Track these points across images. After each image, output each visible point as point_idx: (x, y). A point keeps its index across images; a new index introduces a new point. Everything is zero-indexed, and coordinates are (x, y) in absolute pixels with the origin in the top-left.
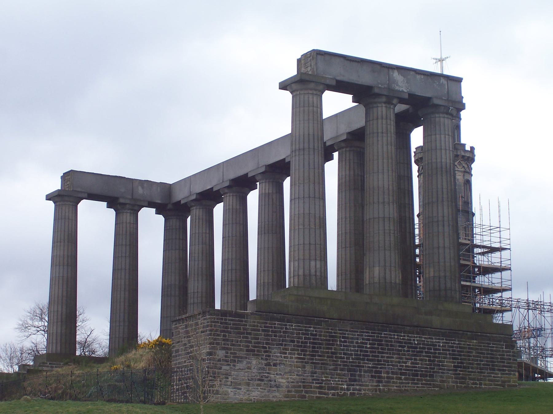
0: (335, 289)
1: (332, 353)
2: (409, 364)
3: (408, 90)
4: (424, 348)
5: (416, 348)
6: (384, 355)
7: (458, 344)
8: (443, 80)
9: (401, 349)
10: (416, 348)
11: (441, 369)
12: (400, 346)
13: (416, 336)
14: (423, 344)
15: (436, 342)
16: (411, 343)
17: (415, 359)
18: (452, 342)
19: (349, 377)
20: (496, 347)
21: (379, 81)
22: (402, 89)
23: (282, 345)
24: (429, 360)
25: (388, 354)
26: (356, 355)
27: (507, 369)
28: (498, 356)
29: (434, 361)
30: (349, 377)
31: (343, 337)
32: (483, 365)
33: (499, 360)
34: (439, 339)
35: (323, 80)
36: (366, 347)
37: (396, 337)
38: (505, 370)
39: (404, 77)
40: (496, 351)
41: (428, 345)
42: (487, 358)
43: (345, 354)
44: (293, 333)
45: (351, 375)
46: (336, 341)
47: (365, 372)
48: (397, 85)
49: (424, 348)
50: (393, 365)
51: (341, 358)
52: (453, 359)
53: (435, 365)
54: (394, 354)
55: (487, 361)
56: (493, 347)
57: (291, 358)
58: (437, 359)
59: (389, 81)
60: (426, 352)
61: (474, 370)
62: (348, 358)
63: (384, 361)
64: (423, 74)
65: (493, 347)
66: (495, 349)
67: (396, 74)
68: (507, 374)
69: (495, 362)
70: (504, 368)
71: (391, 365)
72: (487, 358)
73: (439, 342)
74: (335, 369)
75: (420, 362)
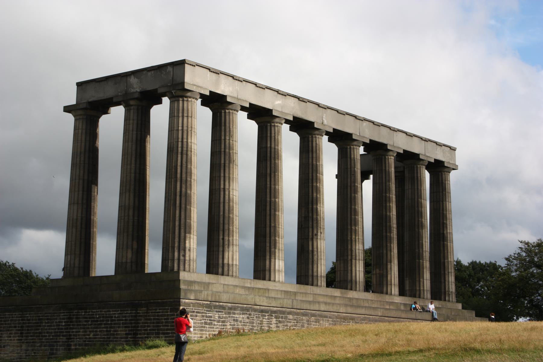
0: (111, 271)
1: (40, 333)
2: (91, 336)
3: (141, 89)
4: (103, 321)
5: (97, 321)
6: (74, 330)
7: (130, 313)
8: (170, 69)
9: (86, 324)
10: (97, 321)
11: (115, 338)
12: (86, 321)
13: (98, 310)
14: (103, 317)
15: (112, 314)
16: (93, 318)
17: (96, 331)
18: (125, 312)
19: (50, 351)
20: (162, 312)
21: (119, 91)
22: (136, 90)
23: (9, 330)
24: (107, 331)
25: (76, 329)
26: (55, 332)
27: (170, 331)
28: (163, 321)
29: (110, 331)
30: (50, 351)
31: (47, 319)
32: (150, 330)
33: (164, 324)
34: (115, 311)
35: (81, 106)
36: (62, 325)
37: (83, 314)
38: (168, 333)
39: (138, 79)
40: (162, 316)
41: (107, 317)
42: (154, 323)
43: (47, 333)
44: (15, 320)
45: (52, 350)
46: (42, 323)
47: (60, 346)
48: (133, 88)
49: (103, 321)
50: (79, 338)
51: (45, 336)
52: (125, 327)
53: (111, 335)
54: (81, 328)
55: (153, 326)
56: (159, 312)
57: (14, 340)
58: (112, 329)
59: (126, 87)
60: (105, 324)
61: (142, 336)
62: (49, 336)
63: (74, 335)
64: (154, 70)
65: (159, 312)
66: (161, 314)
67: (133, 80)
68: (170, 337)
69: (160, 326)
70: (168, 331)
71: (78, 338)
72: (154, 323)
73: (115, 314)
74: (40, 346)
75: (100, 333)
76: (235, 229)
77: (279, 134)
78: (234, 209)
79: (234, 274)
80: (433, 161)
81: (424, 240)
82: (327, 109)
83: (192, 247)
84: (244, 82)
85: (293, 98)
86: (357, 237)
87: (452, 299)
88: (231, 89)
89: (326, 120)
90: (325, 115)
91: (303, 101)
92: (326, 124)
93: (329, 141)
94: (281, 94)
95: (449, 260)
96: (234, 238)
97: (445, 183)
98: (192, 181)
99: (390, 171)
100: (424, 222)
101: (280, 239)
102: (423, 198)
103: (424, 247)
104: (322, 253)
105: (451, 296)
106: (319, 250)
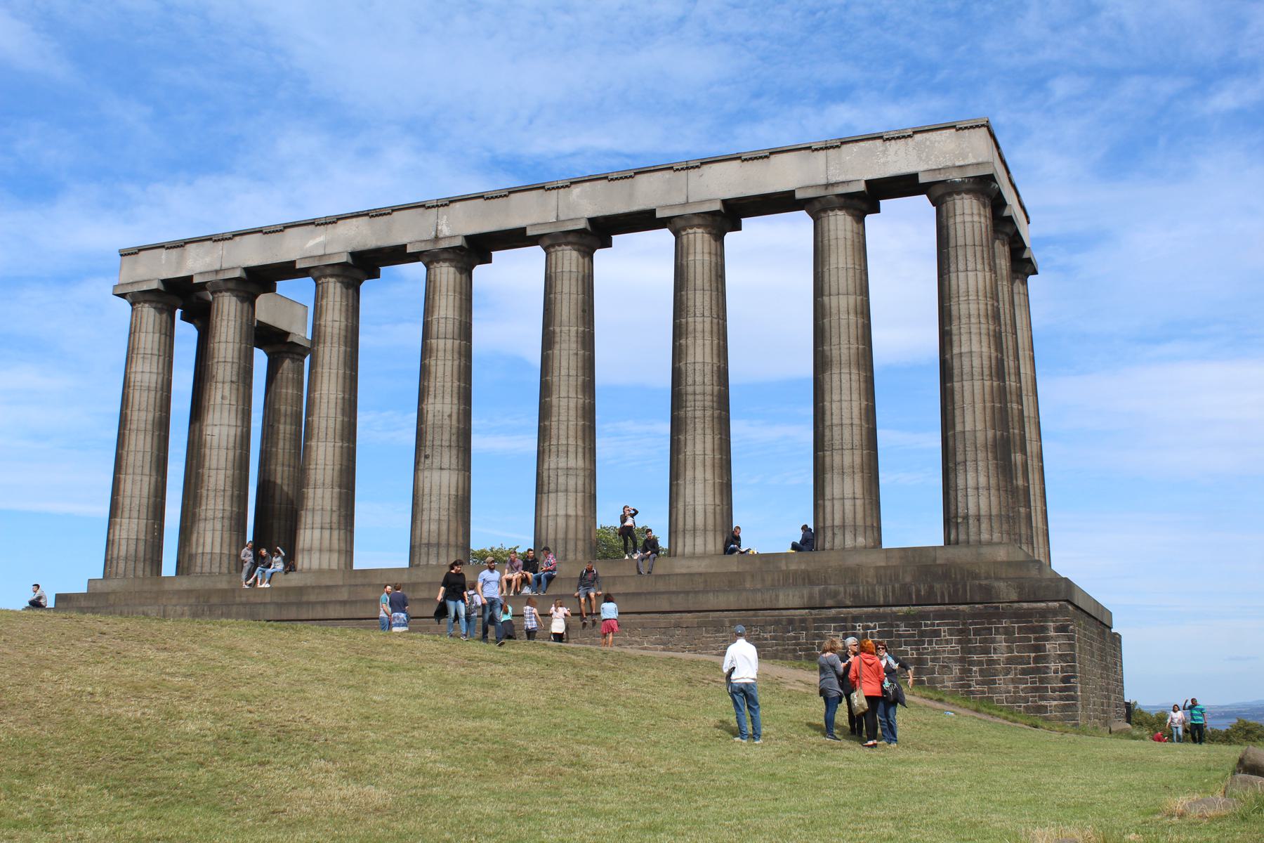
76: (204, 493)
77: (325, 295)
78: (207, 458)
79: (206, 569)
80: (861, 187)
81: (827, 398)
82: (451, 205)
83: (117, 537)
84: (237, 239)
85: (354, 220)
86: (547, 444)
87: (968, 534)
88: (208, 260)
89: (447, 226)
90: (445, 217)
91: (381, 215)
92: (447, 234)
93: (490, 262)
94: (322, 224)
95: (959, 428)
96: (204, 507)
97: (947, 226)
98: (127, 432)
99: (685, 263)
100: (828, 353)
101: (311, 491)
102: (827, 292)
103: (828, 417)
104: (427, 498)
105: (962, 529)
106: (421, 492)
